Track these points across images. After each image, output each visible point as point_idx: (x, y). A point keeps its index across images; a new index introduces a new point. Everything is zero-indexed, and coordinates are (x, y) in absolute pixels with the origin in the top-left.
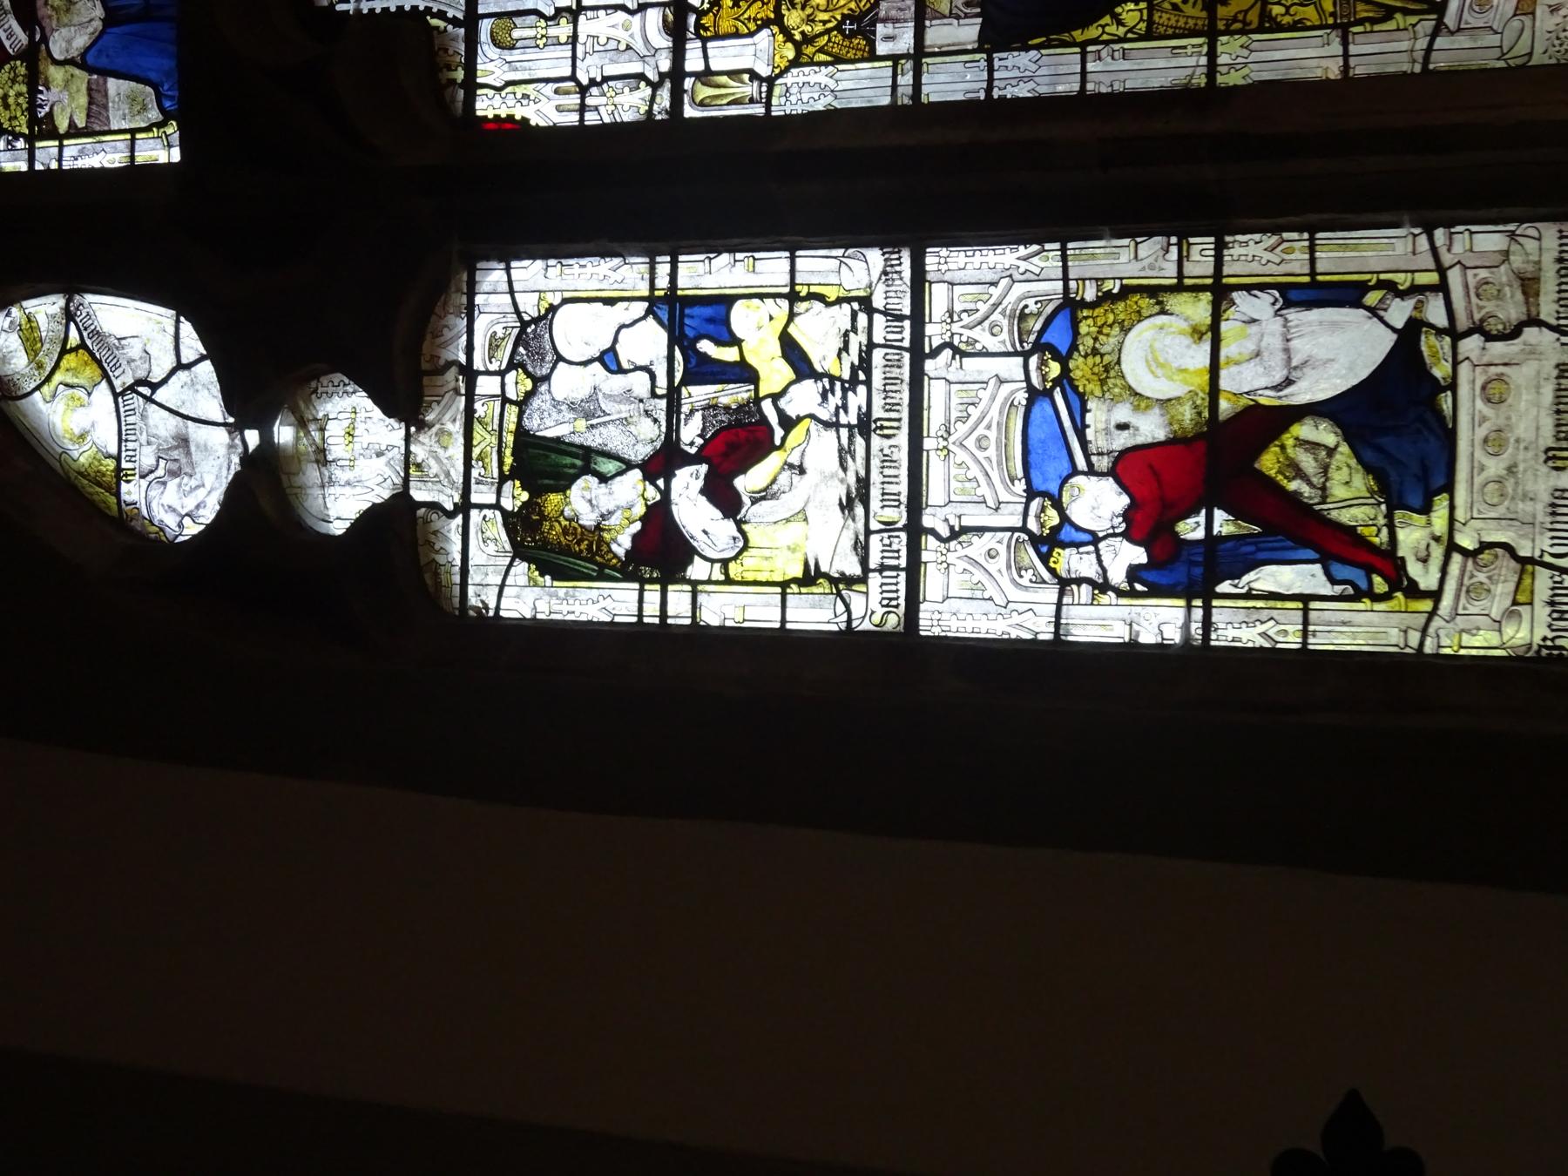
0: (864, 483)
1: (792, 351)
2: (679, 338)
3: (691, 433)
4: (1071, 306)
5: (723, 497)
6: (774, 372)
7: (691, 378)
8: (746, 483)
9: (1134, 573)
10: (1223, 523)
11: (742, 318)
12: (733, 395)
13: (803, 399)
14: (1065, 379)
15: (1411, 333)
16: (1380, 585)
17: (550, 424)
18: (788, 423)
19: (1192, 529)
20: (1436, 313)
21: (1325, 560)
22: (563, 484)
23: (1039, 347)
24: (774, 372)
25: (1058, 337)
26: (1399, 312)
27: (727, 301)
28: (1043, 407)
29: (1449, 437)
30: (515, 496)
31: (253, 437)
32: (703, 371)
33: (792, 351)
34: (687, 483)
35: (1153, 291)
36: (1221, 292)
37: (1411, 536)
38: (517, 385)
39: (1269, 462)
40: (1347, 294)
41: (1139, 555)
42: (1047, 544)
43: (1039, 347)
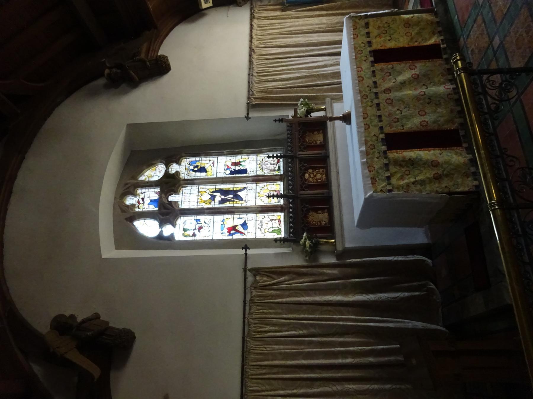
0: (209, 230)
1: (205, 222)
2: (196, 221)
3: (197, 228)
4: (224, 219)
5: (199, 231)
6: (203, 223)
7: (197, 224)
8: (200, 230)
9: (228, 235)
10: (234, 232)
11: (201, 220)
12: (200, 225)
13: (205, 225)
14: (223, 224)
15: (245, 220)
16: (243, 235)
17: (185, 228)
18: (204, 227)
19: (232, 232)
20: (247, 219)
21: (240, 233)
22: (186, 231)
23: (222, 222)
24: (203, 223)
25: (223, 221)
26: (245, 219)
27: (200, 219)
28: (222, 225)
29: (247, 226)
30: (183, 232)
31: (161, 229)
32: (198, 223)
33: (205, 222)
34: (197, 230)
35: (229, 218)
36: (234, 218)
37: (246, 232)
38: (184, 225)
39: (237, 228)
40: (242, 218)
41: (228, 234)
42: (222, 234)
43: (222, 222)
